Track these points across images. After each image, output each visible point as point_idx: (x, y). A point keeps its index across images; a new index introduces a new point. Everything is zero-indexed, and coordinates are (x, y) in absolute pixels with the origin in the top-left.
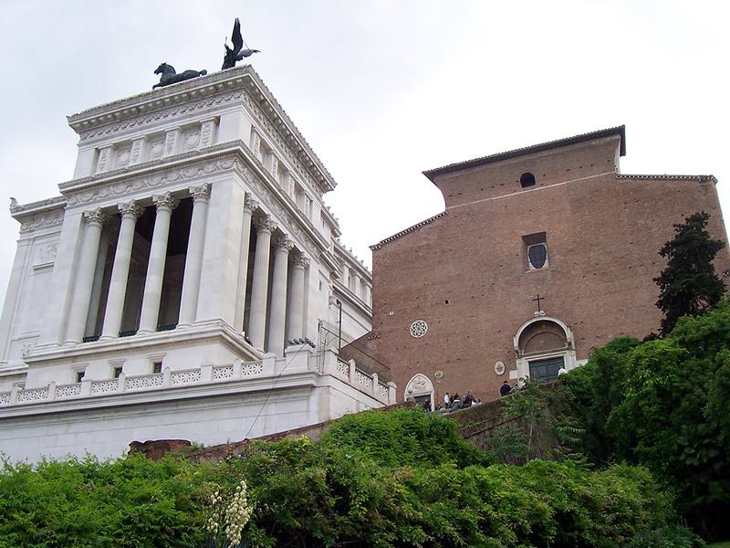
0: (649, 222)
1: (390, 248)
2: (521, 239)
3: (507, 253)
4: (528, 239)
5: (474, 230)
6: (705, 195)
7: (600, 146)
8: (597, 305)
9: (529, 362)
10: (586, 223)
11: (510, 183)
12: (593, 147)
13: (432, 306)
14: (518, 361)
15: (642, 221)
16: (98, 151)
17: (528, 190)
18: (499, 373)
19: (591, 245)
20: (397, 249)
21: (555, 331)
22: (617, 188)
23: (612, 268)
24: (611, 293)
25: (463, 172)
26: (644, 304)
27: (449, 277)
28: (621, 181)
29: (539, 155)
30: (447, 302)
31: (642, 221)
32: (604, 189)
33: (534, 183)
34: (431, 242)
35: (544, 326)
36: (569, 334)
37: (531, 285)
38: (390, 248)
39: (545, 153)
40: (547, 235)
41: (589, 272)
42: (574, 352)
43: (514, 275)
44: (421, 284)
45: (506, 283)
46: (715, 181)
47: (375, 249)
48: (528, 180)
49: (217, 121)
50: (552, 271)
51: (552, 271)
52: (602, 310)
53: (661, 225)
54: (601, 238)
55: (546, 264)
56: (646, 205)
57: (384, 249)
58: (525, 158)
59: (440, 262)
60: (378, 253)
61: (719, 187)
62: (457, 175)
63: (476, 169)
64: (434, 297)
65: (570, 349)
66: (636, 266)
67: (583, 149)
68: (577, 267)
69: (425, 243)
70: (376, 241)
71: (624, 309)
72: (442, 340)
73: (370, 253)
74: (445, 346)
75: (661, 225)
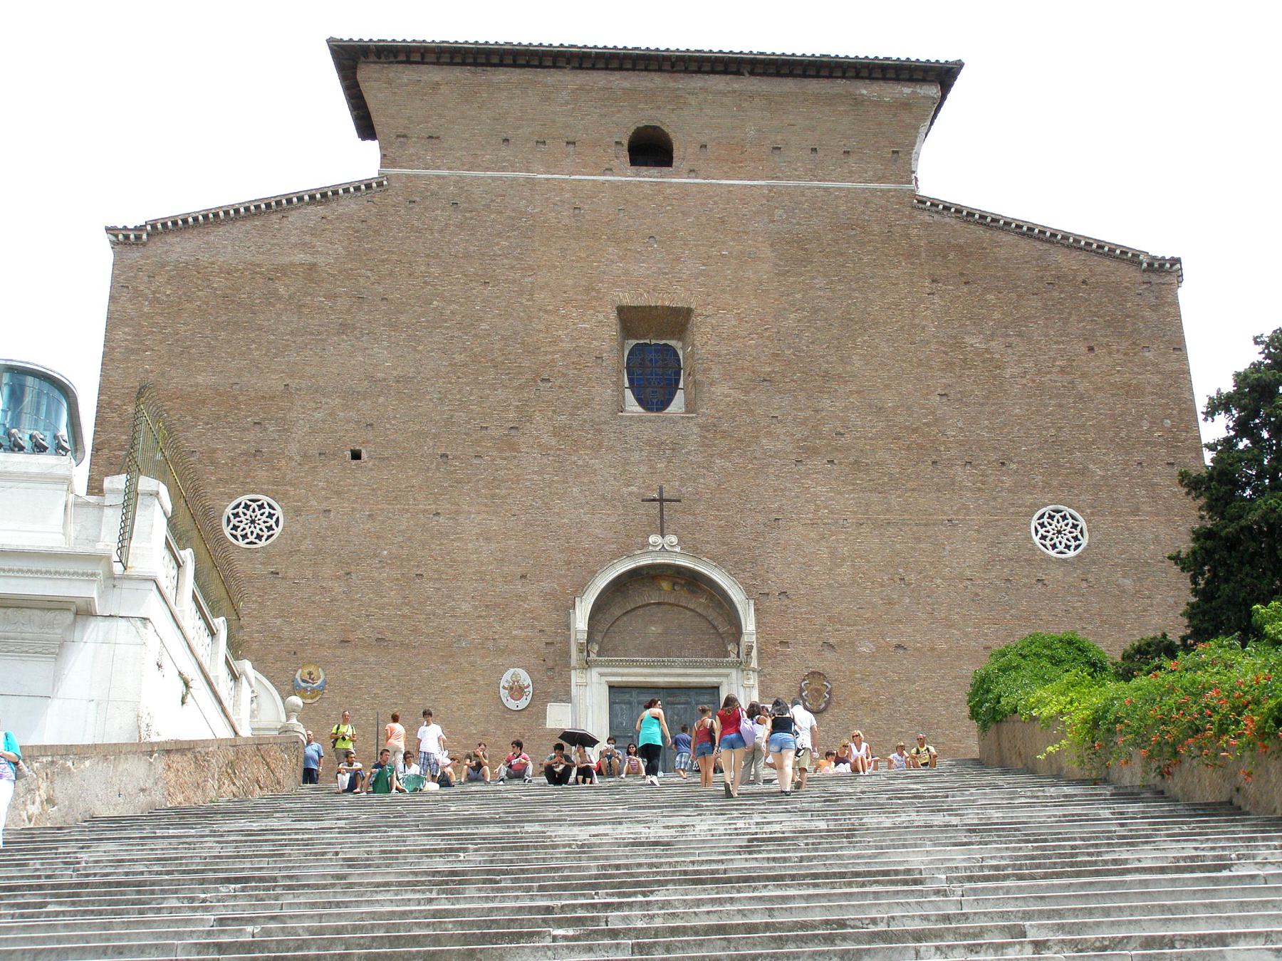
1: (179, 248)
2: (613, 315)
3: (566, 346)
4: (630, 319)
5: (467, 256)
6: (1155, 308)
7: (877, 104)
8: (833, 553)
9: (611, 687)
10: (815, 311)
12: (857, 102)
13: (305, 456)
14: (575, 677)
15: (974, 341)
17: (649, 177)
18: (512, 704)
19: (826, 376)
20: (204, 258)
21: (699, 603)
23: (881, 455)
25: (458, 73)
26: (968, 573)
27: (371, 378)
28: (926, 217)
29: (697, 82)
30: (356, 455)
31: (974, 341)
32: (876, 228)
33: (670, 165)
34: (320, 260)
35: (665, 585)
36: (749, 625)
37: (636, 457)
38: (179, 248)
39: (718, 83)
40: (696, 320)
41: (815, 451)
42: (753, 680)
43: (584, 413)
44: (274, 382)
45: (555, 434)
46: (1179, 275)
47: (123, 239)
50: (703, 427)
51: (703, 427)
52: (845, 569)
54: (858, 363)
55: (677, 404)
56: (988, 297)
57: (157, 248)
58: (656, 81)
59: (344, 328)
60: (135, 255)
61: (1189, 297)
62: (437, 78)
63: (501, 76)
64: (313, 432)
65: (741, 666)
68: (780, 430)
69: (300, 257)
70: (133, 219)
71: (912, 577)
72: (327, 571)
73: (103, 257)
74: (338, 588)
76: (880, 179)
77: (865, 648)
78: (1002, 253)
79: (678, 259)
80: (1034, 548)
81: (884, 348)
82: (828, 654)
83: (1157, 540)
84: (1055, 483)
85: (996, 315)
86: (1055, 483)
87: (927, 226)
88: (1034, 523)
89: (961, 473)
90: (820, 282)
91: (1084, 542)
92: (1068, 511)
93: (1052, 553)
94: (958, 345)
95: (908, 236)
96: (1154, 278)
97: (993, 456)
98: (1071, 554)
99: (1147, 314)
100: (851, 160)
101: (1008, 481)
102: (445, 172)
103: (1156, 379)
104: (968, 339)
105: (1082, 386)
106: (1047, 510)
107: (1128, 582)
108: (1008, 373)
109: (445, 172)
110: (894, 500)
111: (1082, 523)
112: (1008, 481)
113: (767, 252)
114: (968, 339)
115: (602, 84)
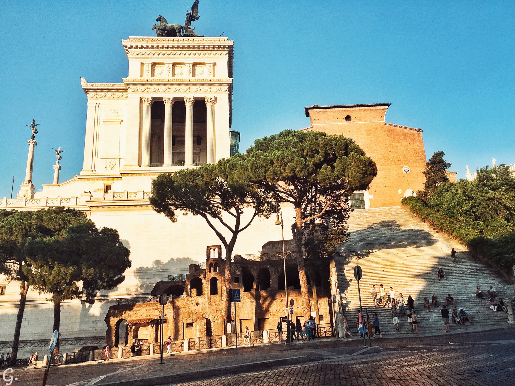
0: (397, 144)
10: (372, 141)
11: (341, 119)
12: (376, 110)
16: (142, 64)
17: (348, 123)
22: (385, 128)
23: (382, 161)
24: (382, 170)
28: (386, 126)
48: (348, 118)
49: (215, 64)
53: (401, 146)
54: (378, 148)
56: (396, 137)
66: (391, 161)
67: (373, 110)
71: (387, 177)
75: (401, 146)
76: (380, 121)
77: (382, 187)
78: (397, 130)
79: (353, 135)
80: (403, 172)
81: (382, 146)
82: (378, 188)
83: (420, 170)
84: (406, 163)
85: (397, 140)
86: (406, 163)
87: (387, 127)
88: (403, 169)
89: (393, 163)
90: (372, 137)
91: (410, 171)
92: (407, 167)
93: (405, 173)
94: (392, 144)
95: (384, 129)
96: (419, 132)
97: (397, 160)
98: (408, 173)
99: (418, 138)
100: (376, 118)
101: (399, 163)
102: (321, 124)
103: (419, 147)
104: (393, 143)
105: (409, 149)
106: (405, 167)
107: (416, 176)
108: (399, 148)
109: (321, 124)
110: (384, 167)
111: (409, 168)
112: (399, 163)
113: (365, 133)
114: (393, 143)
115: (342, 110)
